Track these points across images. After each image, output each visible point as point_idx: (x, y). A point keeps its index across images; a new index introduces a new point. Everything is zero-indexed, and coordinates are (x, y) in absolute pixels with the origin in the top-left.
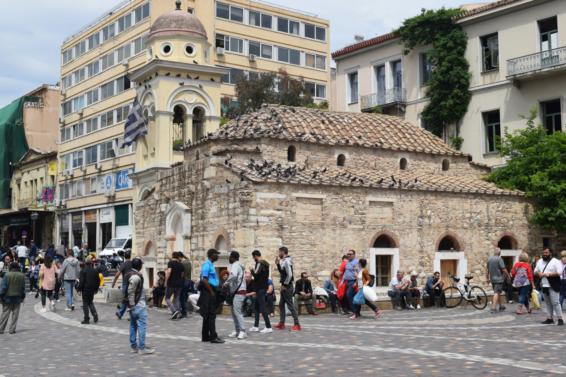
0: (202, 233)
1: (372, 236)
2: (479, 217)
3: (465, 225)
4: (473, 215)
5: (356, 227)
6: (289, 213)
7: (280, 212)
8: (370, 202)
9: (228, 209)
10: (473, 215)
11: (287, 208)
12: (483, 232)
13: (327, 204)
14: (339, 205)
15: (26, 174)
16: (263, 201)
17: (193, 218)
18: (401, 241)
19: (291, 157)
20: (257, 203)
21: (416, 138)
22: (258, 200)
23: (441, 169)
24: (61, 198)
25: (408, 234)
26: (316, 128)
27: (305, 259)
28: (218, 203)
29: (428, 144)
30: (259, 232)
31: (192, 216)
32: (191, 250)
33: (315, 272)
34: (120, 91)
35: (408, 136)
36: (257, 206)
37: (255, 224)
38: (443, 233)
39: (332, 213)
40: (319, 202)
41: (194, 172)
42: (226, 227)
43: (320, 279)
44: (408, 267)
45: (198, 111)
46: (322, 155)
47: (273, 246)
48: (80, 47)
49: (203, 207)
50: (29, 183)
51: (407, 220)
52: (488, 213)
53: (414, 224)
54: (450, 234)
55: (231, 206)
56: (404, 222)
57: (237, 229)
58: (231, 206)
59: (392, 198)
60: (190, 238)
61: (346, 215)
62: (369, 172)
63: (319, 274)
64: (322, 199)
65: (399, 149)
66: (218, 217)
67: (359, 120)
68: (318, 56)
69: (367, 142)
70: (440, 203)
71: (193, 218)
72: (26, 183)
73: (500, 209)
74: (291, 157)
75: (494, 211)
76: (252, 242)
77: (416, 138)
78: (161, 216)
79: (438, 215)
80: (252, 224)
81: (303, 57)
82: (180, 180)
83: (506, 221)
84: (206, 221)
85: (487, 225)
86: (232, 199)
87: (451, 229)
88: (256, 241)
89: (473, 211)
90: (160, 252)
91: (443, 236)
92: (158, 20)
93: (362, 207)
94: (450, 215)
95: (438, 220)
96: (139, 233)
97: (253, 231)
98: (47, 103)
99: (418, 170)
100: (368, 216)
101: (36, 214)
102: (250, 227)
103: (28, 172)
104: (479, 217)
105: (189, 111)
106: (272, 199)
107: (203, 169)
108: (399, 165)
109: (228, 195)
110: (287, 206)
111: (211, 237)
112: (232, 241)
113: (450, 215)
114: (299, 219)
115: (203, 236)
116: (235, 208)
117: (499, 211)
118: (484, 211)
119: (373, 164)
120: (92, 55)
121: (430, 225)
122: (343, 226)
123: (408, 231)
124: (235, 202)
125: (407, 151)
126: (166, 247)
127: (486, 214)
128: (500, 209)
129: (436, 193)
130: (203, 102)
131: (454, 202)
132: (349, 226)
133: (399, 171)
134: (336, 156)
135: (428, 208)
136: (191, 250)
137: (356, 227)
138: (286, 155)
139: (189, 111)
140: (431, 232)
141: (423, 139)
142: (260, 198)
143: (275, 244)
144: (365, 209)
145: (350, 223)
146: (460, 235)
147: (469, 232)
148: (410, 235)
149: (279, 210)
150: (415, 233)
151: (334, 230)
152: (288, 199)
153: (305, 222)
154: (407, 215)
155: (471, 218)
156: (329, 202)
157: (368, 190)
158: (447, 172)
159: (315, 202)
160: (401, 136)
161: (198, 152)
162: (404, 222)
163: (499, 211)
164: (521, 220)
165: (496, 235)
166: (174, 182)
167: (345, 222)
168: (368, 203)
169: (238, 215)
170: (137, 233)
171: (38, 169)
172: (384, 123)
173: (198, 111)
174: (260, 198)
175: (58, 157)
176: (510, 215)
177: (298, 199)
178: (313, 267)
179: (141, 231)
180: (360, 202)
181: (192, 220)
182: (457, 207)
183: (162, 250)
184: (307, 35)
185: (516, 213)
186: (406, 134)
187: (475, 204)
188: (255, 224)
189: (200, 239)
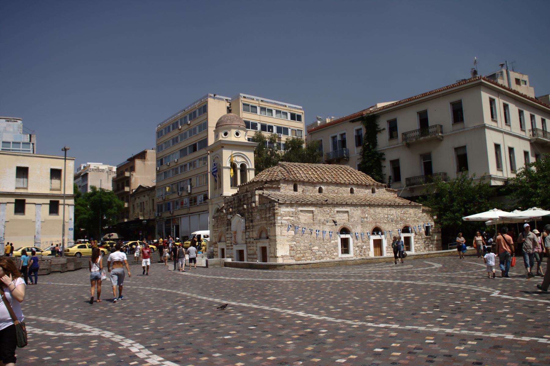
0: (252, 230)
1: (338, 228)
2: (392, 217)
3: (385, 221)
4: (389, 216)
5: (330, 224)
6: (297, 218)
7: (293, 218)
8: (337, 212)
9: (266, 217)
10: (389, 216)
11: (296, 216)
12: (394, 224)
13: (316, 213)
14: (322, 213)
15: (137, 199)
16: (284, 213)
17: (246, 222)
18: (353, 231)
19: (295, 189)
20: (281, 214)
21: (358, 177)
22: (282, 212)
23: (371, 193)
24: (158, 212)
25: (356, 227)
26: (307, 174)
27: (306, 241)
28: (260, 214)
29: (364, 180)
30: (283, 228)
31: (246, 221)
32: (246, 238)
33: (311, 248)
34: (190, 153)
35: (354, 176)
36: (282, 216)
37: (281, 224)
38: (373, 226)
39: (318, 218)
40: (311, 212)
41: (246, 198)
43: (313, 251)
44: (357, 243)
45: (243, 166)
46: (311, 188)
47: (290, 235)
48: (168, 129)
50: (139, 204)
51: (356, 219)
52: (396, 214)
53: (360, 221)
54: (377, 226)
55: (268, 215)
56: (354, 221)
58: (268, 215)
59: (348, 209)
60: (245, 232)
61: (325, 218)
62: (335, 195)
63: (313, 248)
64: (313, 211)
65: (349, 183)
66: (260, 221)
67: (328, 168)
68: (298, 130)
69: (333, 180)
70: (372, 210)
71: (246, 222)
72: (137, 204)
73: (402, 212)
74: (295, 189)
75: (399, 214)
76: (279, 234)
77: (358, 177)
79: (371, 217)
80: (279, 224)
81: (290, 131)
82: (238, 202)
83: (406, 218)
84: (254, 224)
85: (396, 221)
86: (268, 213)
87: (378, 224)
88: (281, 233)
89: (388, 214)
90: (228, 240)
91: (374, 227)
92: (220, 119)
93: (333, 214)
94: (377, 217)
95: (371, 219)
96: (215, 231)
97: (279, 228)
98: (147, 159)
99: (360, 194)
100: (336, 218)
101: (145, 221)
102: (278, 226)
103: (139, 198)
104: (392, 217)
105: (238, 166)
106: (288, 211)
108: (350, 191)
109: (266, 210)
110: (296, 215)
111: (257, 232)
112: (269, 233)
113: (377, 217)
114: (302, 221)
115: (253, 231)
116: (270, 216)
117: (402, 213)
118: (394, 214)
119: (336, 191)
120: (174, 133)
121: (367, 222)
122: (323, 223)
123: (356, 225)
124: (270, 214)
125: (353, 184)
126: (231, 237)
127: (395, 215)
128: (402, 212)
129: (370, 205)
130: (245, 161)
131: (379, 210)
132: (327, 224)
133: (350, 194)
134: (318, 188)
135: (366, 213)
136: (246, 238)
137: (330, 224)
138: (292, 188)
139: (238, 166)
140: (368, 226)
141: (361, 177)
142: (283, 211)
143: (291, 234)
144: (335, 215)
145: (327, 222)
146: (383, 227)
147: (387, 224)
148: (358, 227)
149: (292, 217)
150: (360, 226)
151: (319, 226)
152: (296, 211)
153: (305, 222)
154: (356, 217)
155: (388, 217)
156: (316, 212)
157: (335, 205)
158: (374, 194)
159: (310, 212)
160: (350, 176)
161: (247, 188)
162: (354, 221)
163: (402, 213)
164: (414, 217)
165: (401, 226)
166: (235, 203)
167: (325, 222)
168: (336, 212)
170: (214, 231)
171: (144, 196)
172: (340, 169)
173: (243, 166)
174: (283, 211)
175: (156, 189)
176: (408, 215)
177: (301, 211)
178: (310, 245)
179: (216, 229)
180: (332, 212)
181: (246, 223)
182: (381, 212)
183: (228, 239)
184: (291, 119)
185: (411, 214)
186: (353, 175)
187: (390, 210)
188: (281, 224)
189: (251, 233)
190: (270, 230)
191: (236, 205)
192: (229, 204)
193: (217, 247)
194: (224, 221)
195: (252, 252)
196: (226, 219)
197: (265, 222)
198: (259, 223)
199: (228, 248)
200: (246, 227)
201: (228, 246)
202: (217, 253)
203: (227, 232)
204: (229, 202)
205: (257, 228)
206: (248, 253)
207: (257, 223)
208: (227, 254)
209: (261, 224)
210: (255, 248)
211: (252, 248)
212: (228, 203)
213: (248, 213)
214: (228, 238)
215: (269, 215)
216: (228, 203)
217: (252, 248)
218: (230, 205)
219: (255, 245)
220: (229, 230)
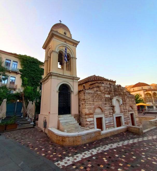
0: (125, 105)
58: (132, 100)
86: (132, 98)
90: (106, 111)
116: (133, 100)
179: (92, 103)
183: (107, 110)
191: (113, 90)
192: (106, 87)
193: (93, 117)
194: (100, 97)
195: (126, 117)
199: (107, 116)
201: (106, 115)
202: (91, 123)
203: (105, 105)
205: (128, 105)
208: (106, 121)
210: (128, 114)
211: (126, 114)
214: (106, 109)
218: (106, 89)
219: (128, 113)
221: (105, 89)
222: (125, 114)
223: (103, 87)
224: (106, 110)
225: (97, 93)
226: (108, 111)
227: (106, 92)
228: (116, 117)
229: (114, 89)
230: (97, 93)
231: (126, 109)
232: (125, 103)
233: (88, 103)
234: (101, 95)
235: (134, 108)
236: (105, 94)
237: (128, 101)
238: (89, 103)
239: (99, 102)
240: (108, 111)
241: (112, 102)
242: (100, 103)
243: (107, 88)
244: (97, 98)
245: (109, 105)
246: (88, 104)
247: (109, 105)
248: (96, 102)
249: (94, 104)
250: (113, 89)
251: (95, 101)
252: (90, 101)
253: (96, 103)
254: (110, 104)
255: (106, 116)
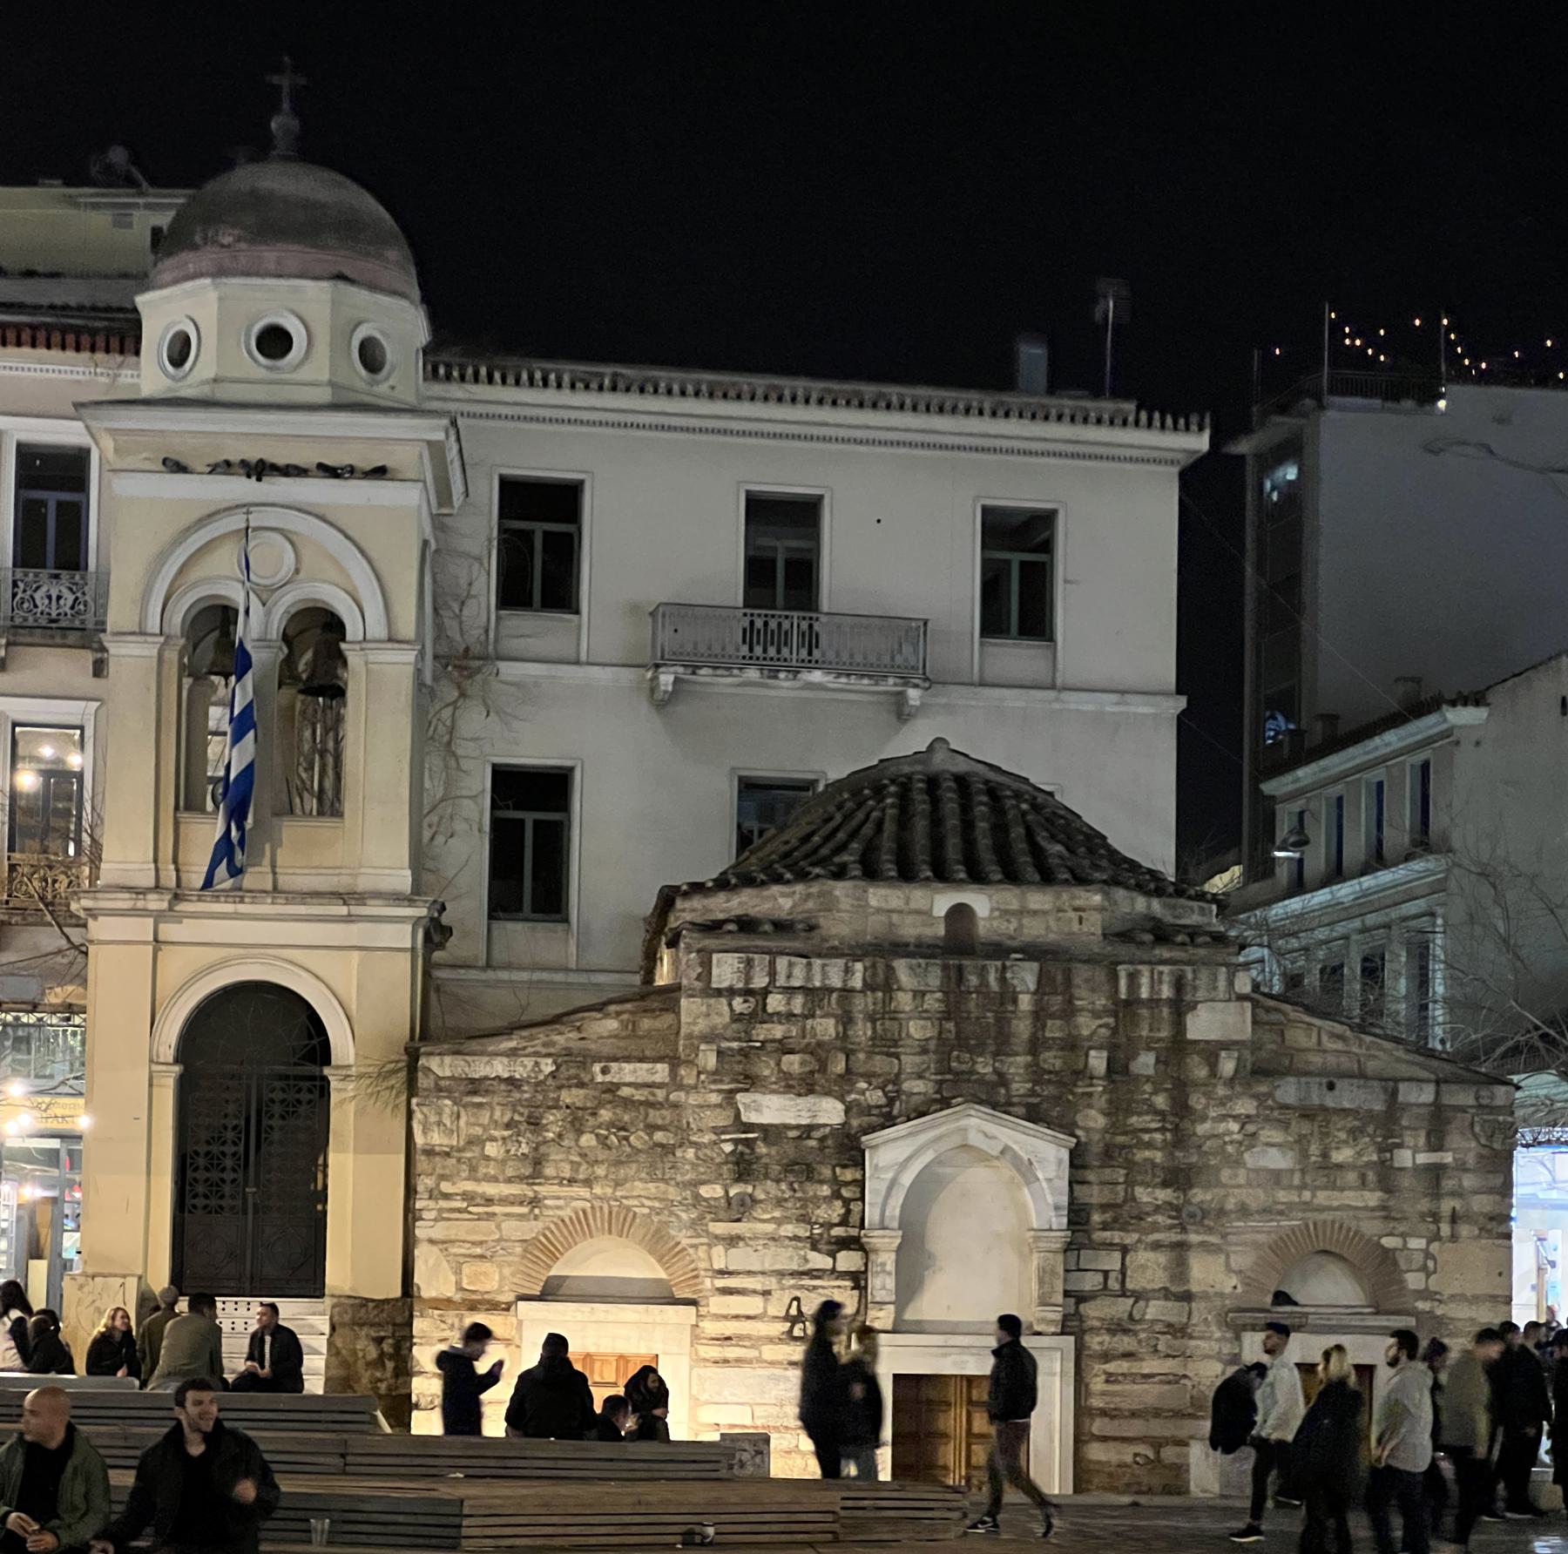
17: (1091, 1176)
42: (1371, 1227)
49: (1180, 1139)
55: (1404, 1158)
57: (1454, 1237)
66: (1303, 1187)
78: (747, 1142)
84: (1199, 1195)
107: (1180, 1007)
111: (1243, 1259)
112: (1414, 1281)
116: (1435, 1172)
136: (1067, 1294)
169: (1454, 1194)
190: (1428, 1255)
192: (775, 1002)
194: (652, 1128)
196: (723, 1119)
197: (1373, 1198)
198: (1282, 1196)
200: (1077, 1215)
203: (720, 1228)
204: (789, 991)
206: (1096, 1402)
207: (1256, 1198)
209: (1307, 1206)
212: (765, 992)
213: (1118, 1109)
214: (722, 1273)
215: (1423, 1158)
216: (765, 992)
217: (1150, 1366)
218: (790, 1016)
220: (758, 1213)
221: (760, 1015)
222: (1128, 1355)
223: (731, 992)
224: (721, 1283)
225: (608, 1078)
226: (766, 1293)
227: (766, 1068)
228: (895, 1376)
229: (952, 1010)
230: (599, 1078)
231: (1187, 1297)
232: (1175, 1209)
233: (446, 1187)
234: (676, 1106)
235: (1426, 1294)
236: (750, 1082)
237: (1276, 1178)
238: (468, 1197)
239: (618, 1184)
240: (766, 1293)
241: (861, 1184)
242: (642, 1193)
243: (798, 1004)
244: (587, 1140)
245: (803, 1231)
246: (447, 1196)
247: (803, 1231)
248: (572, 1181)
249: (535, 1202)
250: (933, 1002)
251: (549, 1171)
252: (473, 1175)
253: (583, 1192)
254: (836, 1211)
255: (715, 1352)
